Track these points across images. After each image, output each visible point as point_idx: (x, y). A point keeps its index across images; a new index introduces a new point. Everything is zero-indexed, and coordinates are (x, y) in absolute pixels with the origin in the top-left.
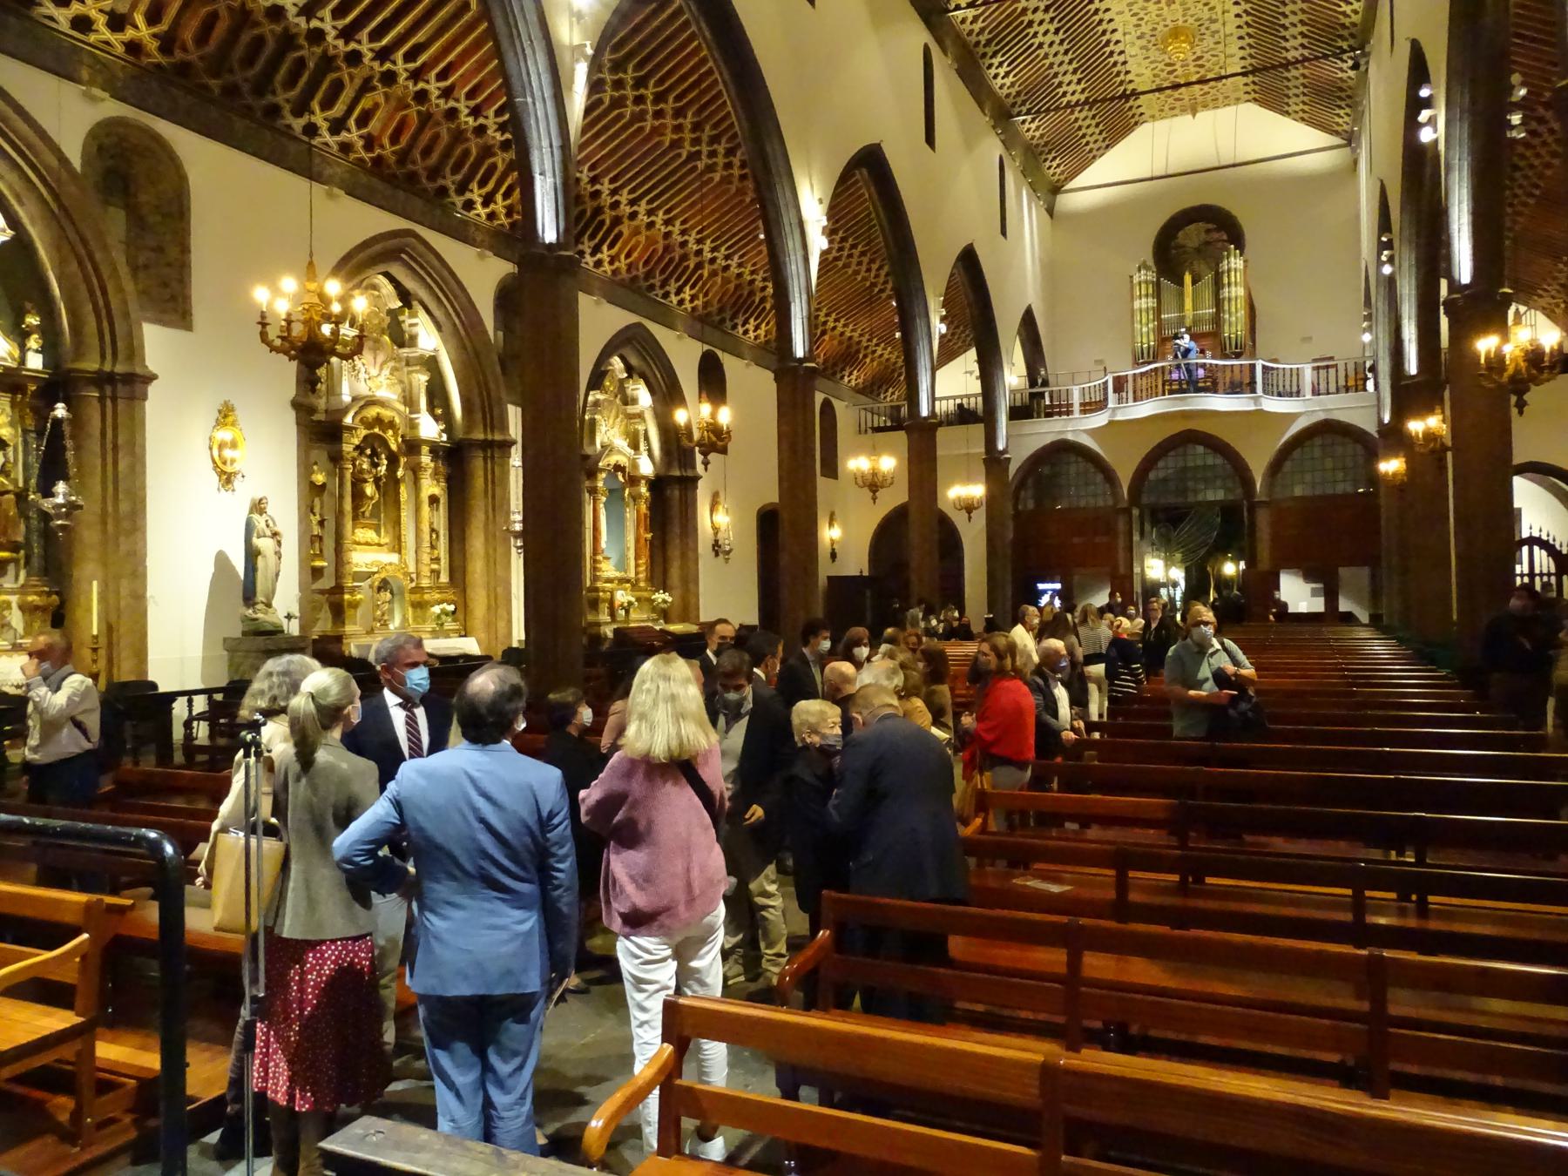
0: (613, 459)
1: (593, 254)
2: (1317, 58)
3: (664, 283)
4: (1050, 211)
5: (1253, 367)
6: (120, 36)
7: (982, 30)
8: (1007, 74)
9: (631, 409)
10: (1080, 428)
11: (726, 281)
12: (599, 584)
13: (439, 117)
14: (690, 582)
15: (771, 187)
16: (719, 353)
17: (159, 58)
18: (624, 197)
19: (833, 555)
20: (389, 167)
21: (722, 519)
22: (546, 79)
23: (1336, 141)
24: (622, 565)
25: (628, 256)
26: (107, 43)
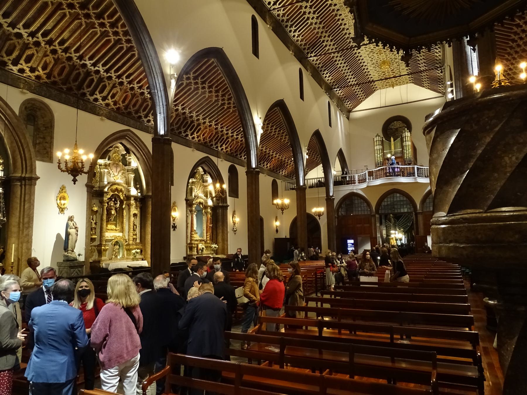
0: (198, 200)
1: (191, 135)
2: (430, 70)
3: (216, 144)
4: (348, 118)
5: (413, 168)
6: (33, 74)
7: (320, 63)
8: (329, 76)
9: (205, 184)
10: (358, 188)
11: (237, 142)
12: (193, 242)
13: (138, 95)
14: (225, 240)
15: (244, 114)
16: (236, 166)
17: (47, 80)
18: (201, 117)
19: (277, 231)
20: (122, 110)
21: (237, 220)
22: (161, 85)
23: (440, 95)
24: (201, 235)
25: (203, 135)
26: (29, 76)
